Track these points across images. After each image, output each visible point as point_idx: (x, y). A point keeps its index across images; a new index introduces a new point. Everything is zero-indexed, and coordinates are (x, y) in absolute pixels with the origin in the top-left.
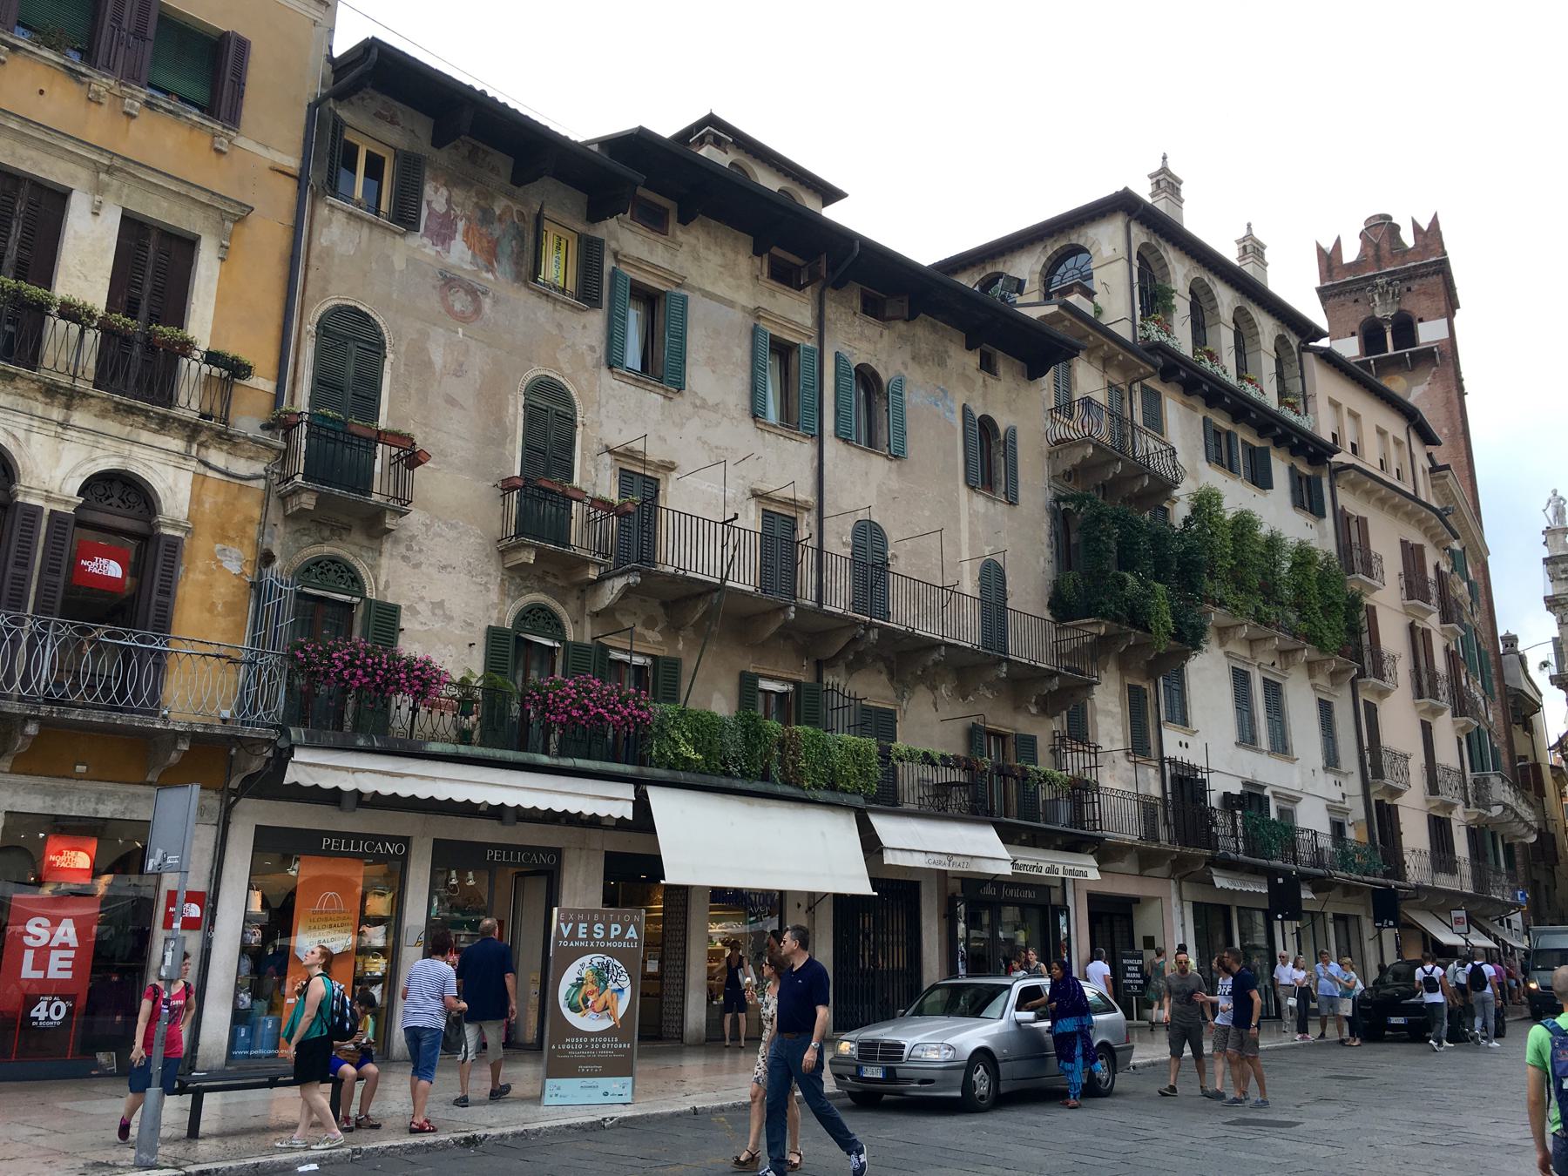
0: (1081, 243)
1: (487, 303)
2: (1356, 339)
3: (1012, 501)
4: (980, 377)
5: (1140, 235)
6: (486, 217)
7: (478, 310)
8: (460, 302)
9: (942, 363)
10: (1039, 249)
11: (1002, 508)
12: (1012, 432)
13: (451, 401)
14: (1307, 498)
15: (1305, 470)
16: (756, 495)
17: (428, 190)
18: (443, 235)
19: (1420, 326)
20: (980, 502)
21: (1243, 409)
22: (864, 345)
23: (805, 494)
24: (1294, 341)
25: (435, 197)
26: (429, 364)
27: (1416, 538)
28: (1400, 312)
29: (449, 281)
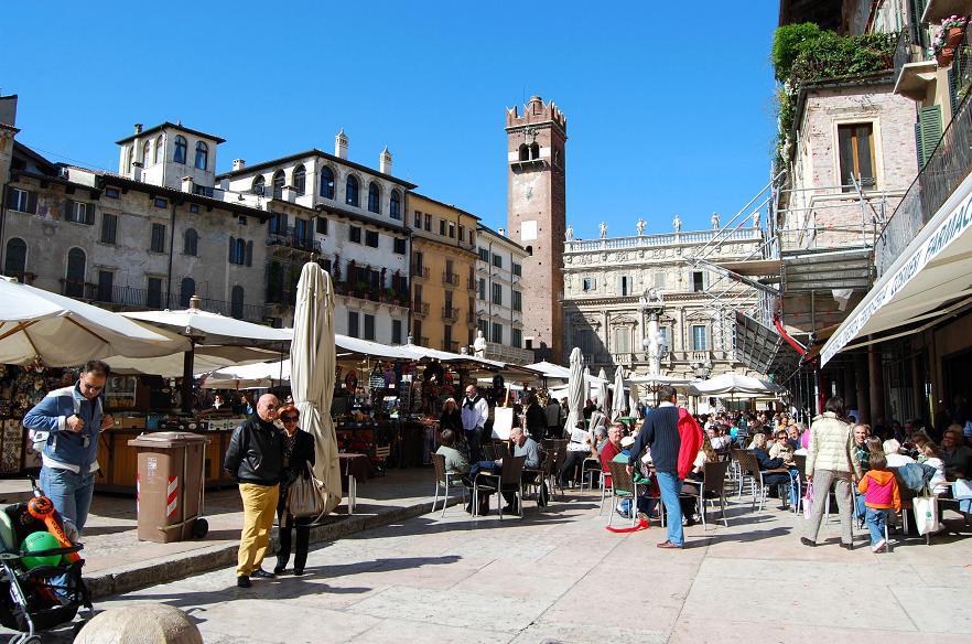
1: (57, 229)
3: (249, 264)
5: (323, 162)
6: (58, 205)
7: (54, 232)
8: (48, 231)
9: (222, 224)
12: (251, 243)
14: (399, 248)
17: (39, 201)
18: (44, 211)
19: (541, 150)
20: (235, 268)
24: (403, 189)
25: (41, 202)
26: (39, 250)
29: (45, 225)
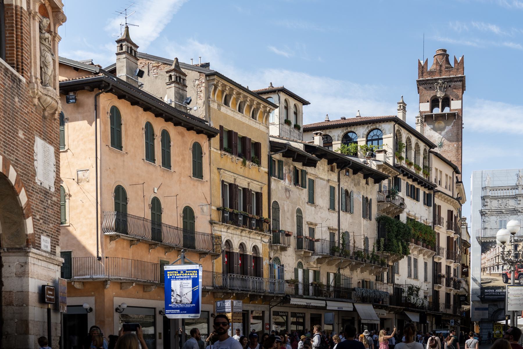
0: (380, 128)
2: (429, 104)
4: (365, 186)
10: (366, 126)
11: (369, 221)
12: (371, 200)
13: (288, 218)
14: (428, 202)
15: (427, 192)
16: (329, 228)
20: (365, 221)
21: (415, 179)
22: (346, 184)
23: (336, 227)
24: (428, 148)
26: (285, 211)
27: (452, 208)
28: (445, 95)
29: (287, 190)
